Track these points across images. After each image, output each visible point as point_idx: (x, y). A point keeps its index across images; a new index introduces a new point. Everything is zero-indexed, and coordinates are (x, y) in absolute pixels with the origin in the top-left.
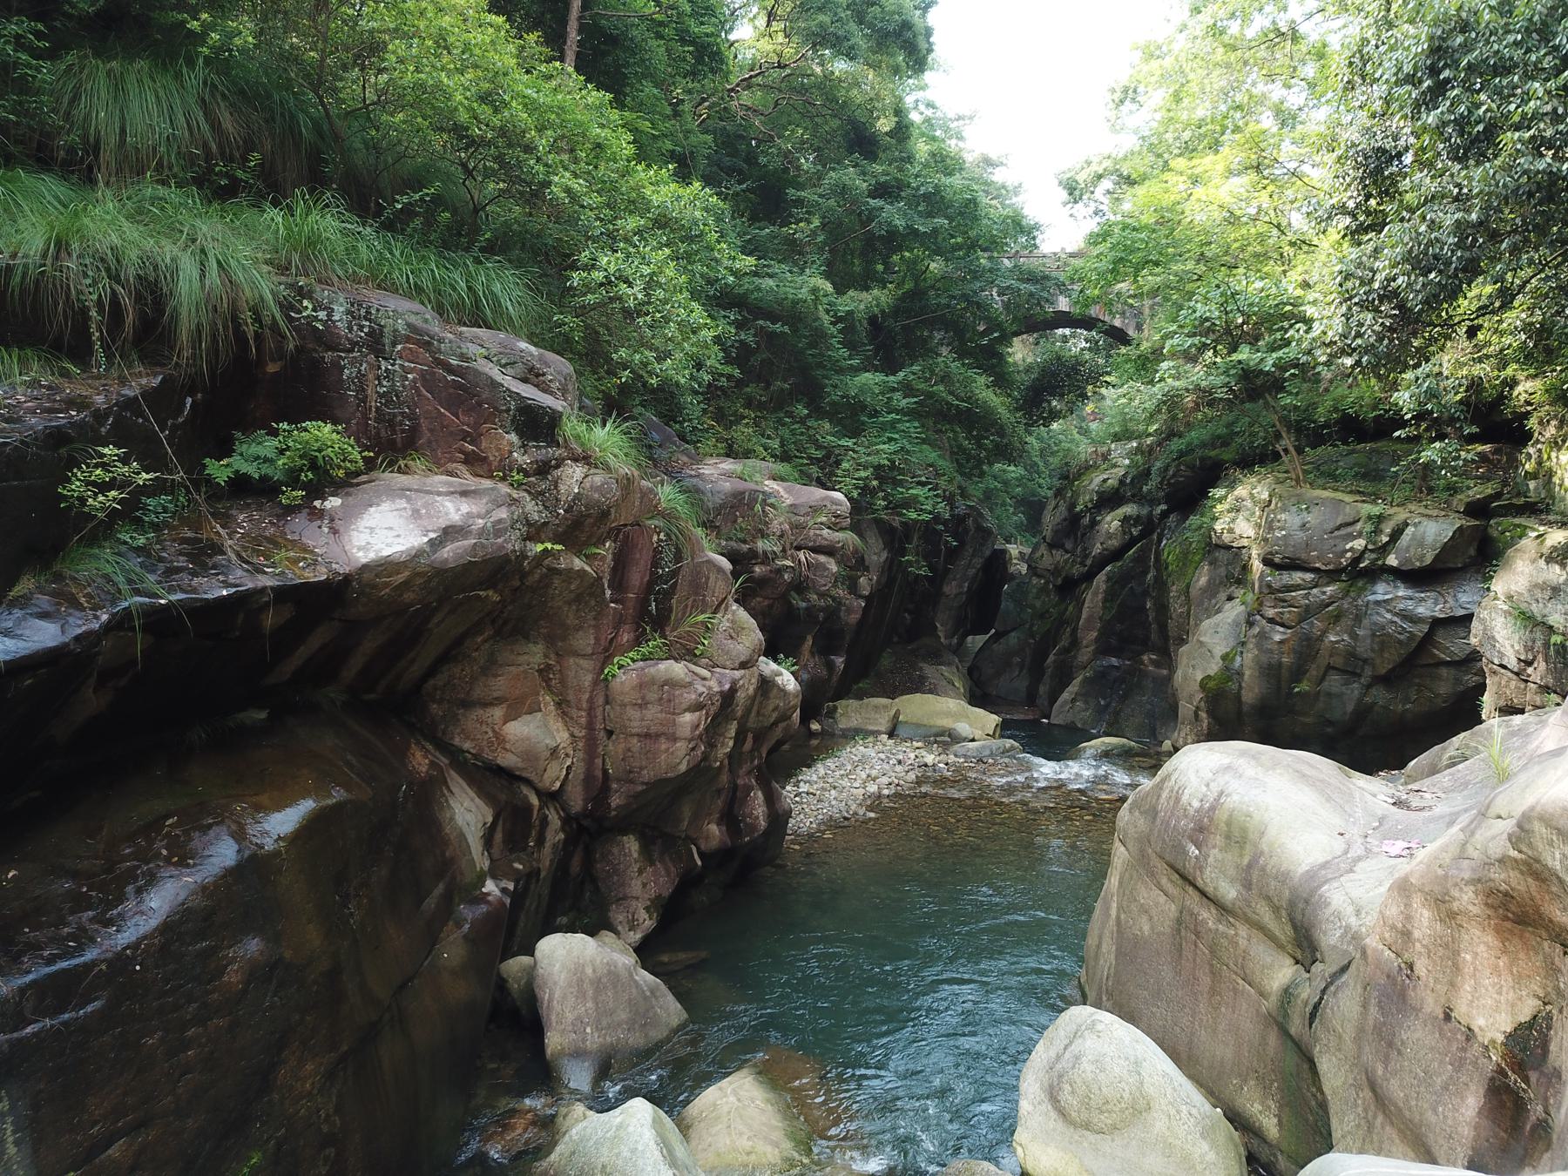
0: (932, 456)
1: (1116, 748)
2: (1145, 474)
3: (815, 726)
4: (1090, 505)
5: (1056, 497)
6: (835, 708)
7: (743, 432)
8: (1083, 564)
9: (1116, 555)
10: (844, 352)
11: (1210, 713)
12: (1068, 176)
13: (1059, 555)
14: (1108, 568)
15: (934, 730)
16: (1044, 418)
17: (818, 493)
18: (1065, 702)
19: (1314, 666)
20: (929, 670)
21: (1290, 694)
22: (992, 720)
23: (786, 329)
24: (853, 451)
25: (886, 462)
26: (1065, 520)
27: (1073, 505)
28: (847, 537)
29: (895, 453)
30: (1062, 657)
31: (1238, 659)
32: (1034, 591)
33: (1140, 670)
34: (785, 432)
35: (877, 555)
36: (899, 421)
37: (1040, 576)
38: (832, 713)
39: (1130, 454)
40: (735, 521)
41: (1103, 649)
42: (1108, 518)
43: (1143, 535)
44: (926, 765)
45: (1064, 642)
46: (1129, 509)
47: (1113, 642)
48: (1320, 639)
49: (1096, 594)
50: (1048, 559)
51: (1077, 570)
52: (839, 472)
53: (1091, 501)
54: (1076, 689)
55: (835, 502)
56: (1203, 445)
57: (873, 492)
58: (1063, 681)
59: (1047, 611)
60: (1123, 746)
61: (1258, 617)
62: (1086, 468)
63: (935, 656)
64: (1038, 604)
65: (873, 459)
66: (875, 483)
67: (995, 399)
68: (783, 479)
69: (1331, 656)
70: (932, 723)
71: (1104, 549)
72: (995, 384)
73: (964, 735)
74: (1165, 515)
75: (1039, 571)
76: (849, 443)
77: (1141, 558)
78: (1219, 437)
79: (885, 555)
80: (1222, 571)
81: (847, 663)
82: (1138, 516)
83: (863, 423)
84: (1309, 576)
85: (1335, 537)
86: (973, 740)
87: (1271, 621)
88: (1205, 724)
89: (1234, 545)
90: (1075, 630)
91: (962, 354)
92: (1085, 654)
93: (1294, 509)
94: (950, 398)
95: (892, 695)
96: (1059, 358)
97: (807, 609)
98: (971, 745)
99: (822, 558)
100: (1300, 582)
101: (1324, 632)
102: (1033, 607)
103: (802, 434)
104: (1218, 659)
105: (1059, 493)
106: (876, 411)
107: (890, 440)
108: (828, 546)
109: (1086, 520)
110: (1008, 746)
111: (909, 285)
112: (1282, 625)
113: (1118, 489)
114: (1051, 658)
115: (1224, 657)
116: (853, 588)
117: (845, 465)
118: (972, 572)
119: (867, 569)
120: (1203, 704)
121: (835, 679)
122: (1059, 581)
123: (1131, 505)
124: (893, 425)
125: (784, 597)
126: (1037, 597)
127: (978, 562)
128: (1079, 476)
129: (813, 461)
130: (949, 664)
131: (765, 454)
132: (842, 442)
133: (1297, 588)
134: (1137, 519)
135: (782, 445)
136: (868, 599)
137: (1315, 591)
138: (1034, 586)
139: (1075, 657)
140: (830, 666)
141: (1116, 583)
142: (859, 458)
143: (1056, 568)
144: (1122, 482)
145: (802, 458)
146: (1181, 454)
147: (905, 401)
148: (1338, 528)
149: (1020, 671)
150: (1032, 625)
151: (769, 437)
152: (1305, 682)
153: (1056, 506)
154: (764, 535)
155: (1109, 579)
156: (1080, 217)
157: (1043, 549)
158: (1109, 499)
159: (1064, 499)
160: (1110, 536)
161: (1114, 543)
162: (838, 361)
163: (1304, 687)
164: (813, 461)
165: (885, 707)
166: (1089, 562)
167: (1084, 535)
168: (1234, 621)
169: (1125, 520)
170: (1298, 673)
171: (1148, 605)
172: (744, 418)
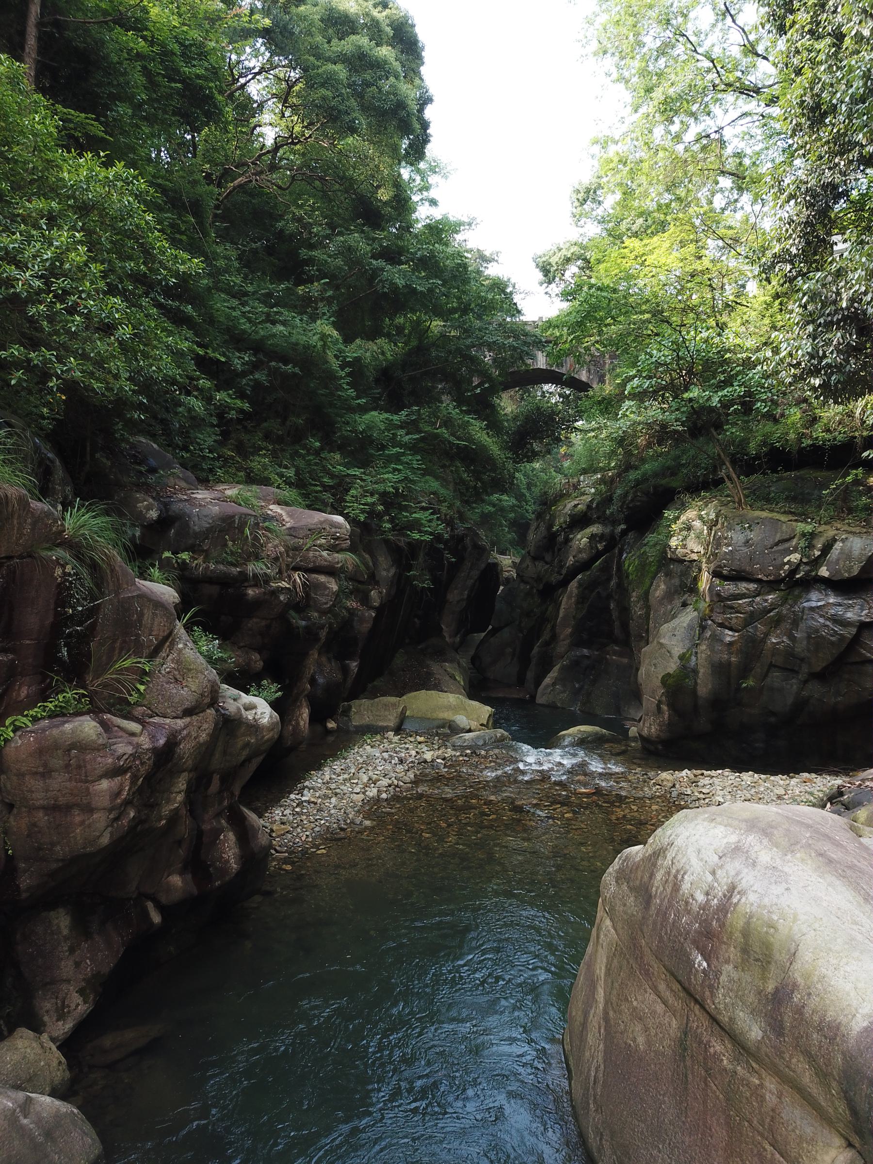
0: (434, 485)
1: (590, 736)
2: (607, 500)
3: (331, 725)
4: (564, 526)
6: (350, 707)
7: (259, 462)
8: (559, 573)
9: (583, 566)
10: (352, 392)
11: (671, 706)
12: (544, 259)
13: (540, 565)
14: (580, 576)
15: (436, 723)
17: (318, 517)
18: (547, 686)
19: (758, 665)
20: (435, 668)
21: (738, 689)
22: (486, 710)
23: (297, 370)
24: (362, 480)
25: (391, 490)
26: (545, 538)
27: (551, 526)
28: (345, 559)
29: (400, 482)
31: (693, 658)
34: (300, 462)
35: (386, 570)
36: (403, 454)
37: (526, 583)
38: (347, 712)
39: (594, 485)
40: (226, 545)
41: (577, 642)
42: (579, 536)
43: (607, 549)
44: (425, 761)
45: (546, 636)
46: (595, 529)
48: (764, 640)
49: (570, 598)
50: (533, 569)
51: (554, 578)
52: (348, 498)
53: (565, 522)
54: (556, 674)
55: (337, 526)
56: (656, 475)
57: (380, 516)
58: (545, 667)
60: (596, 734)
61: (710, 622)
62: (561, 496)
63: (440, 654)
65: (380, 487)
66: (380, 508)
67: (488, 439)
68: (286, 504)
69: (773, 655)
70: (435, 715)
71: (576, 561)
72: (488, 427)
73: (462, 726)
74: (624, 533)
76: (357, 472)
77: (606, 569)
78: (668, 468)
79: (393, 571)
80: (676, 581)
81: (360, 667)
83: (372, 455)
84: (752, 586)
85: (775, 552)
86: (470, 731)
87: (721, 625)
88: (666, 716)
89: (686, 559)
90: (553, 627)
91: (460, 401)
92: (562, 646)
93: (738, 528)
94: (452, 438)
95: (400, 694)
96: (538, 408)
97: (306, 628)
98: (468, 736)
99: (322, 578)
100: (745, 591)
101: (767, 635)
103: (316, 464)
104: (676, 658)
105: (539, 516)
106: (382, 444)
107: (395, 470)
108: (327, 567)
109: (561, 538)
110: (499, 735)
111: (414, 343)
112: (731, 629)
114: (536, 650)
115: (682, 657)
116: (365, 600)
117: (353, 492)
118: (470, 582)
119: (377, 583)
120: (664, 698)
121: (350, 681)
122: (541, 587)
123: (596, 525)
124: (397, 458)
125: (283, 617)
127: (475, 574)
129: (326, 488)
130: (451, 661)
131: (280, 481)
132: (351, 472)
133: (742, 596)
134: (602, 537)
135: (297, 473)
136: (378, 610)
137: (758, 599)
140: (345, 670)
141: (586, 588)
142: (366, 486)
144: (589, 507)
145: (316, 485)
146: (638, 483)
147: (407, 437)
148: (777, 544)
151: (286, 467)
152: (751, 679)
153: (538, 527)
154: (257, 558)
155: (580, 584)
156: (553, 295)
157: (528, 562)
158: (580, 521)
160: (580, 551)
161: (584, 556)
162: (346, 400)
163: (750, 682)
164: (326, 488)
165: (394, 705)
166: (564, 571)
167: (559, 550)
168: (688, 625)
169: (592, 537)
170: (745, 671)
171: (612, 606)
172: (261, 449)
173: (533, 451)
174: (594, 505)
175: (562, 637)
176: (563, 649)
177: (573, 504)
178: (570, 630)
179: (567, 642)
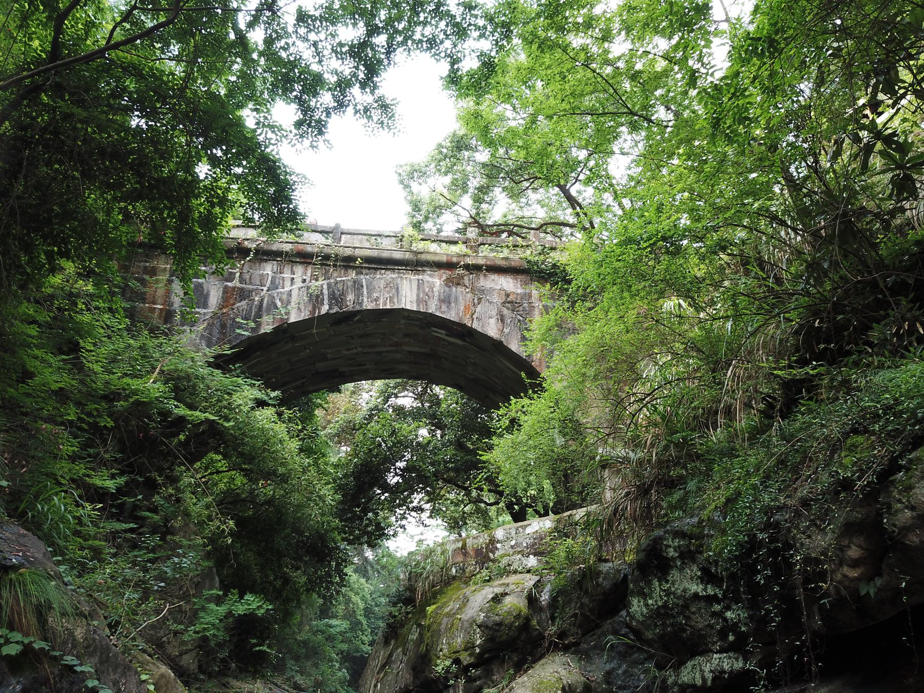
4: (466, 659)
5: (387, 642)
16: (369, 534)
27: (422, 662)
53: (469, 647)
113: (528, 619)
128: (432, 596)
153: (388, 662)
159: (405, 642)
174: (545, 597)
177: (489, 592)
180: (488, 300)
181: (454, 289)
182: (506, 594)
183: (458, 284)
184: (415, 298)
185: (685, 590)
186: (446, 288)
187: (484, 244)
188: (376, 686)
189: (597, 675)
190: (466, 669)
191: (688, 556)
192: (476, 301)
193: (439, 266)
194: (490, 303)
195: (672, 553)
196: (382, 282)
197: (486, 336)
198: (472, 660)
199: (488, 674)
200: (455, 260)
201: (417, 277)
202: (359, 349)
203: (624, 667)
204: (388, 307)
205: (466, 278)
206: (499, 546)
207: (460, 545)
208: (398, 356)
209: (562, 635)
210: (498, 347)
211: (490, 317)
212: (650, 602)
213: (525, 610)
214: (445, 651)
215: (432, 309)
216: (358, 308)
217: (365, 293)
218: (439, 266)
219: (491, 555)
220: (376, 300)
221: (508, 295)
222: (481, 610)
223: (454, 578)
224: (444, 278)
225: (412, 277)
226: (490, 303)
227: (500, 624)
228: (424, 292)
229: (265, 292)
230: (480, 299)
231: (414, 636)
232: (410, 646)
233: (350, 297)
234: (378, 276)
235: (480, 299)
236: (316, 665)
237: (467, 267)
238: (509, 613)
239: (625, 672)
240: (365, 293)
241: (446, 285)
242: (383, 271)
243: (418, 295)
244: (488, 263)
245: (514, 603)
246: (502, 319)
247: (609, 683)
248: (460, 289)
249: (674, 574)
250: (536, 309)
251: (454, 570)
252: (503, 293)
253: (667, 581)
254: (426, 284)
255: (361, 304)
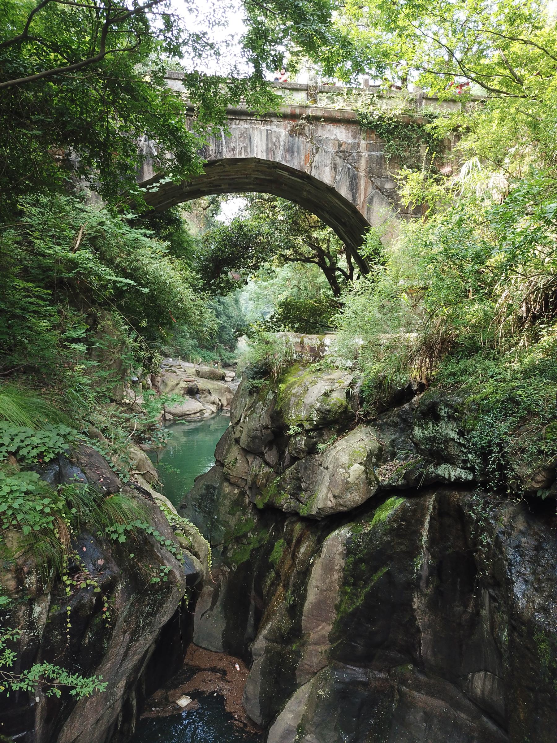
4: (307, 426)
13: (256, 463)
16: (222, 289)
18: (288, 733)
26: (266, 428)
30: (279, 647)
32: (227, 502)
33: (400, 692)
47: (360, 647)
49: (328, 569)
53: (310, 420)
59: (245, 535)
64: (232, 522)
67: (172, 273)
75: (232, 480)
82: (380, 449)
102: (226, 524)
113: (346, 407)
126: (231, 513)
138: (225, 497)
139: (298, 654)
143: (254, 483)
149: (214, 603)
150: (226, 549)
160: (347, 486)
171: (416, 603)
173: (228, 282)
175: (313, 636)
176: (315, 660)
178: (328, 628)
179: (324, 648)
180: (324, 149)
181: (297, 139)
182: (333, 390)
183: (300, 134)
184: (265, 147)
185: (447, 434)
186: (290, 138)
187: (322, 92)
188: (245, 418)
189: (386, 442)
190: (308, 431)
191: (451, 418)
192: (314, 151)
193: (285, 117)
194: (326, 152)
195: (443, 413)
196: (237, 132)
197: (322, 183)
198: (311, 427)
199: (321, 435)
200: (298, 111)
201: (266, 127)
202: (217, 178)
203: (403, 437)
204: (243, 156)
205: (306, 128)
206: (326, 348)
207: (299, 340)
208: (247, 181)
209: (367, 414)
210: (331, 190)
211: (326, 166)
212: (426, 432)
213: (345, 403)
214: (294, 418)
215: (279, 159)
216: (219, 157)
217: (224, 143)
218: (285, 117)
219: (321, 353)
220: (233, 150)
221: (340, 145)
222: (317, 400)
223: (295, 360)
224: (289, 128)
225: (262, 128)
226: (326, 152)
227: (329, 411)
228: (272, 141)
229: (142, 142)
230: (318, 149)
231: (271, 396)
232: (268, 402)
233: (212, 147)
234: (234, 126)
235: (318, 149)
236: (175, 339)
237: (308, 118)
238: (335, 404)
239: (403, 441)
240: (224, 143)
241: (291, 135)
242: (238, 122)
243: (267, 145)
244: (326, 115)
245: (338, 397)
246: (335, 167)
247: (393, 447)
248: (302, 139)
249: (443, 424)
250: (363, 158)
251: (295, 356)
252: (337, 142)
253: (438, 426)
254: (273, 134)
255: (221, 153)
